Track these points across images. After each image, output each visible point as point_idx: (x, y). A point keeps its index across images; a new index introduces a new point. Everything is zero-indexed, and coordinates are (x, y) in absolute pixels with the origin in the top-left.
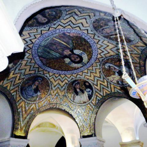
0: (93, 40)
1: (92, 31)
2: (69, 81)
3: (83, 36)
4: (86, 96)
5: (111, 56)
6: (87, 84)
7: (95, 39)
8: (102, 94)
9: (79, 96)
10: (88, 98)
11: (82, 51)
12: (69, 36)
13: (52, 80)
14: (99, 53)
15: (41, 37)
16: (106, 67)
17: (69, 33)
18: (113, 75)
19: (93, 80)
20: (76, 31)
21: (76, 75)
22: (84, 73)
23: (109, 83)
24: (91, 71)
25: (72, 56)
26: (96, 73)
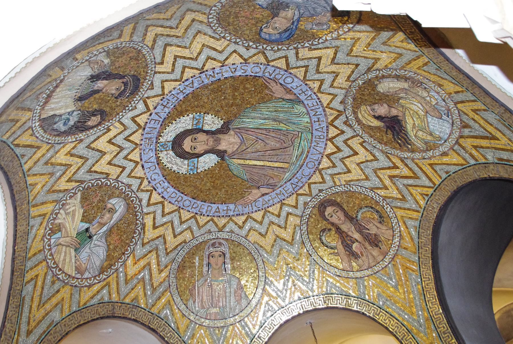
0: (208, 216)
1: (232, 232)
2: (155, 73)
3: (232, 206)
5: (143, 228)
6: (94, 120)
7: (208, 221)
12: (259, 188)
14: (166, 203)
15: (317, 163)
16: (113, 201)
17: (263, 195)
18: (83, 216)
19: (92, 146)
20: (255, 209)
21: (151, 103)
22: (134, 127)
23: (61, 195)
24: (125, 152)
25: (211, 143)
26: (110, 163)
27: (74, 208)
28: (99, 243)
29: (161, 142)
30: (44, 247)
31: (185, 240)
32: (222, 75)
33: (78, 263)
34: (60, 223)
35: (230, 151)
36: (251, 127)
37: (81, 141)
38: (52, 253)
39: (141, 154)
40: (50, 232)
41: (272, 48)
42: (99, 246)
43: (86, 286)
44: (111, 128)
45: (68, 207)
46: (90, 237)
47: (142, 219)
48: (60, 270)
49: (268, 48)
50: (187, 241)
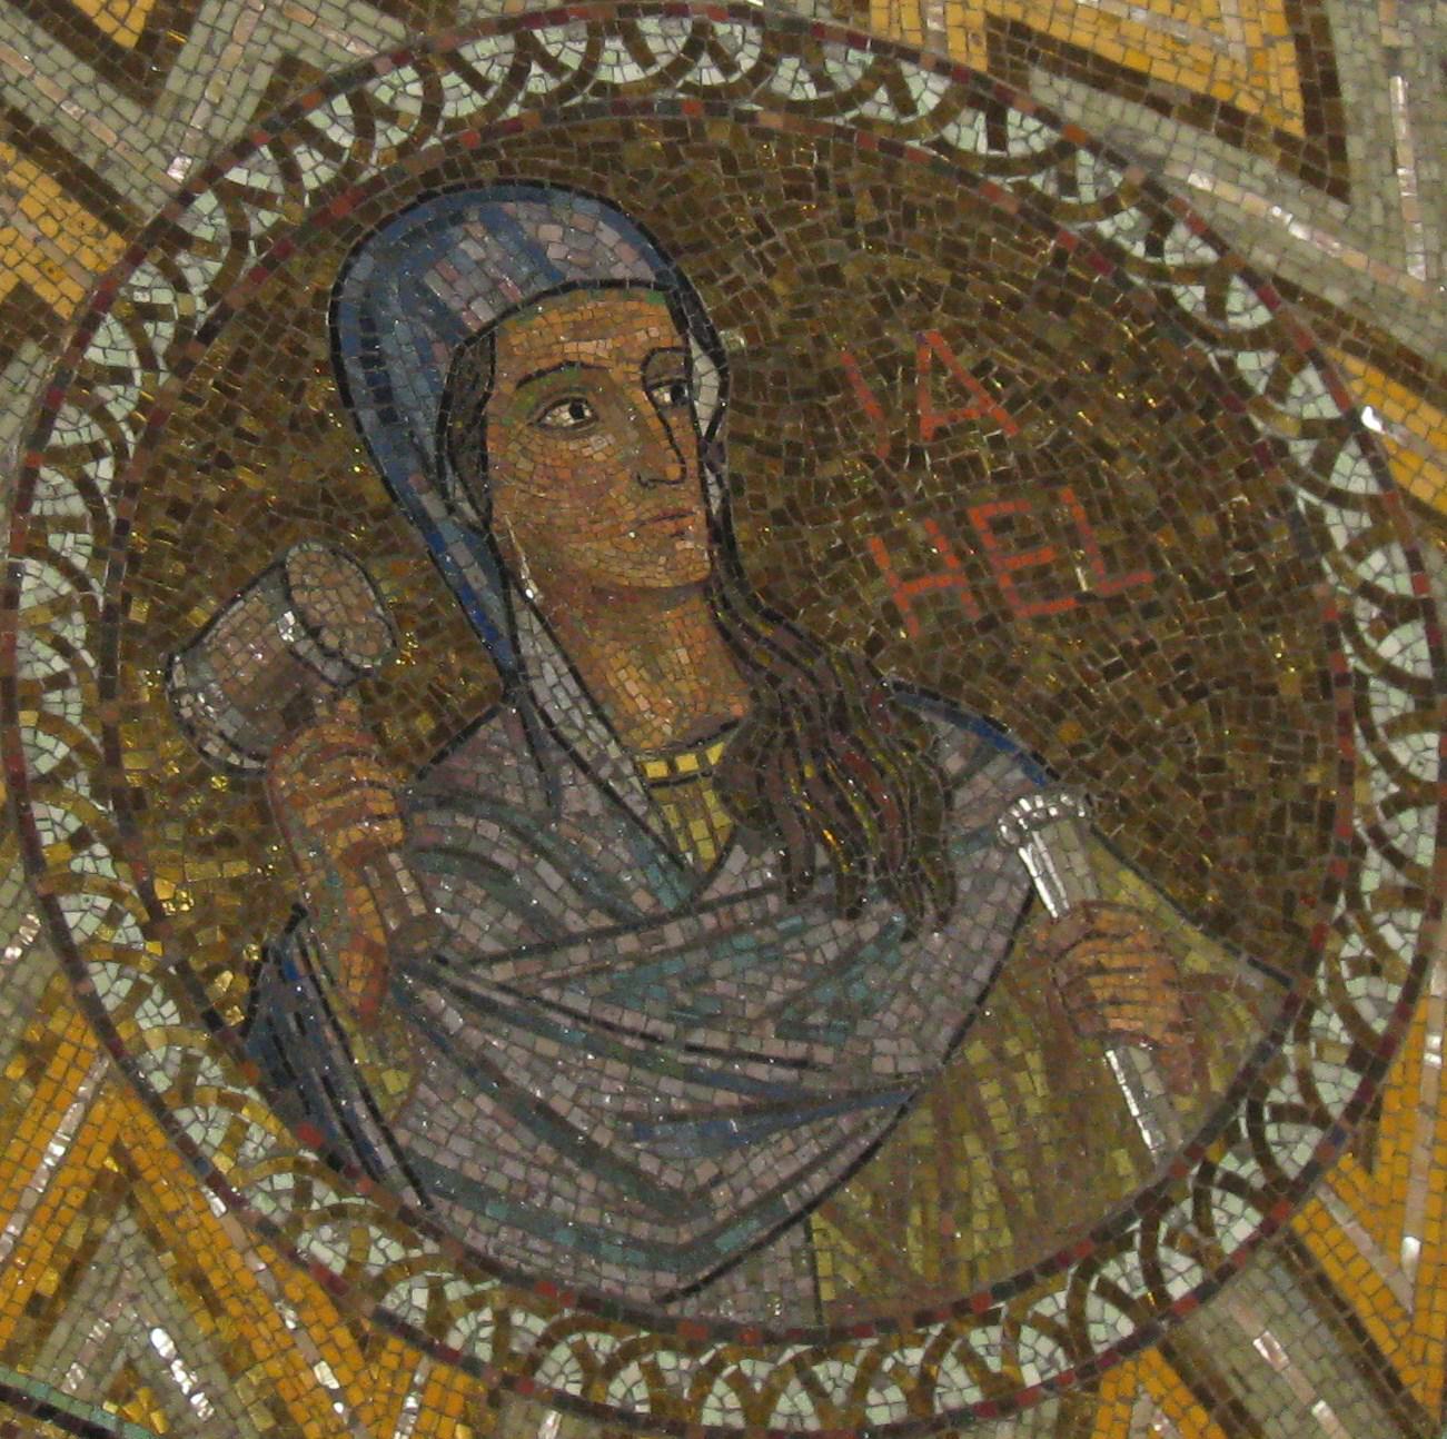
41: (366, 116)
49: (402, 88)
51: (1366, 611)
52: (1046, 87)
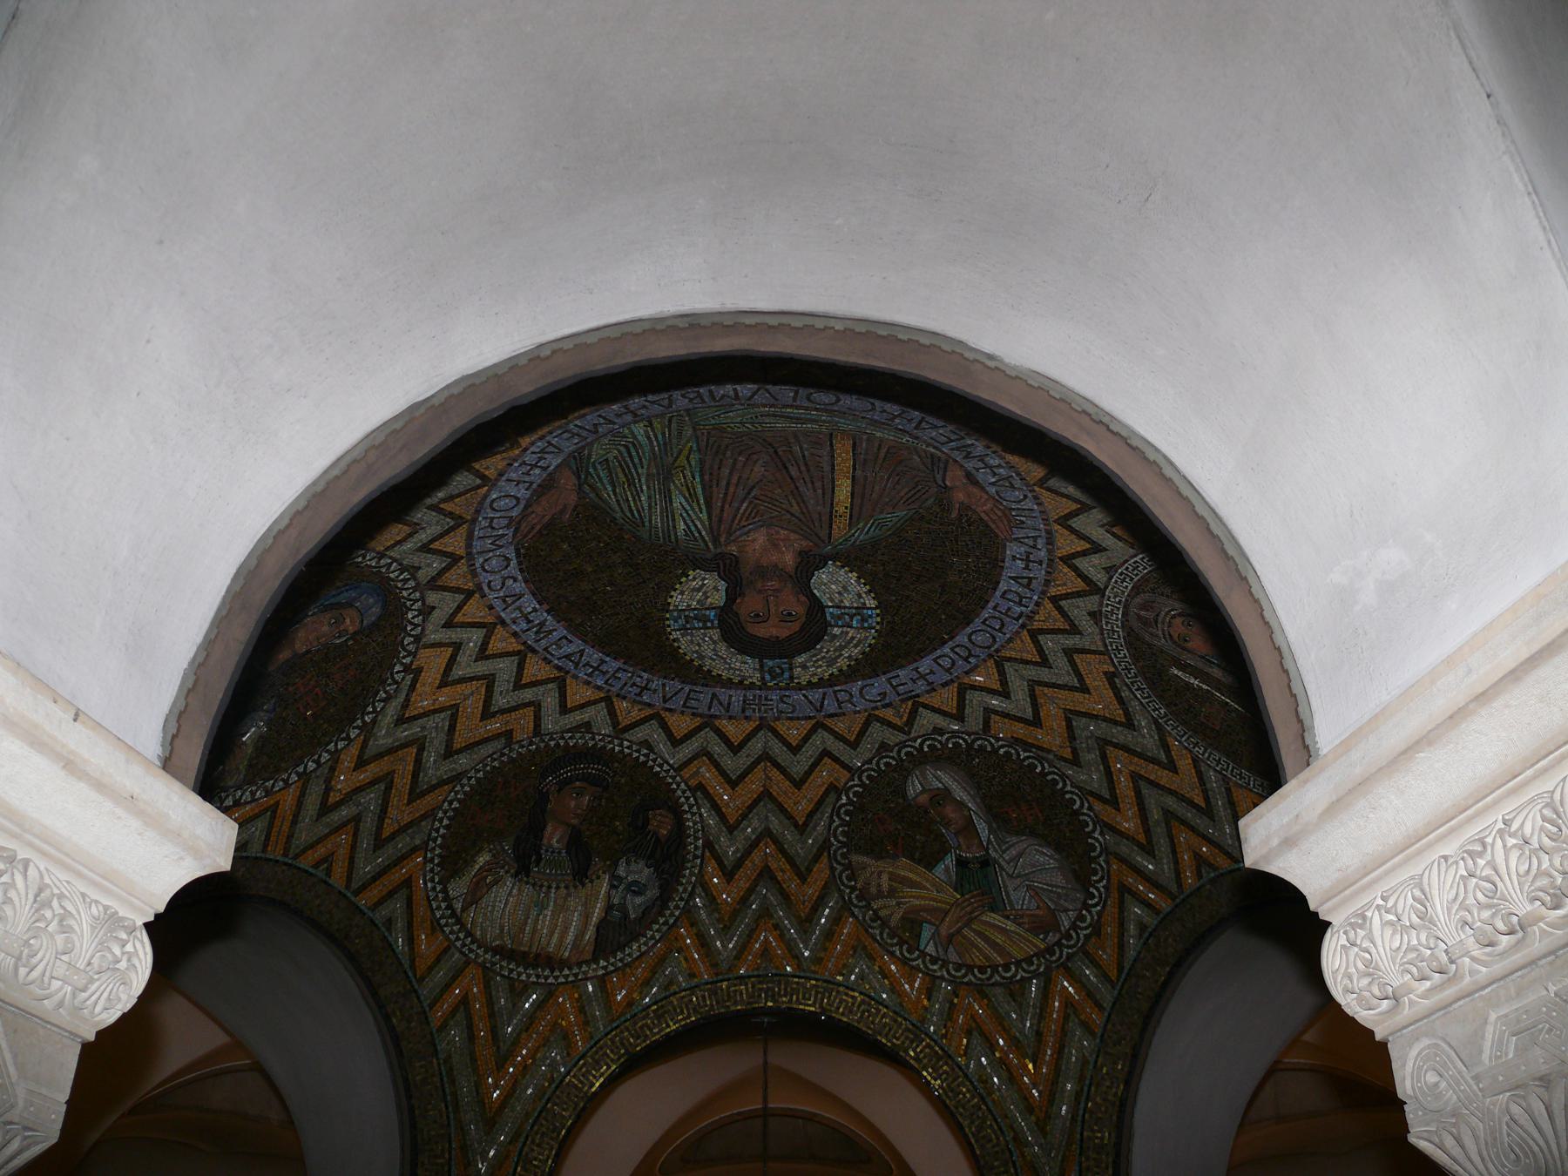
3: (1012, 549)
4: (586, 917)
5: (1027, 746)
6: (661, 825)
8: (725, 946)
9: (528, 890)
10: (590, 934)
11: (870, 603)
13: (433, 663)
16: (914, 787)
18: (919, 862)
27: (885, 877)
28: (1014, 852)
29: (763, 678)
30: (928, 974)
31: (1105, 673)
32: (535, 610)
33: (1026, 920)
34: (903, 918)
35: (800, 544)
36: (704, 516)
37: (709, 845)
38: (954, 963)
39: (791, 719)
40: (905, 947)
42: (1020, 855)
43: (1087, 937)
44: (693, 783)
45: (873, 890)
46: (985, 863)
47: (998, 739)
48: (1007, 967)
49: (412, 583)
50: (1112, 669)
51: (316, 757)
52: (409, 678)
